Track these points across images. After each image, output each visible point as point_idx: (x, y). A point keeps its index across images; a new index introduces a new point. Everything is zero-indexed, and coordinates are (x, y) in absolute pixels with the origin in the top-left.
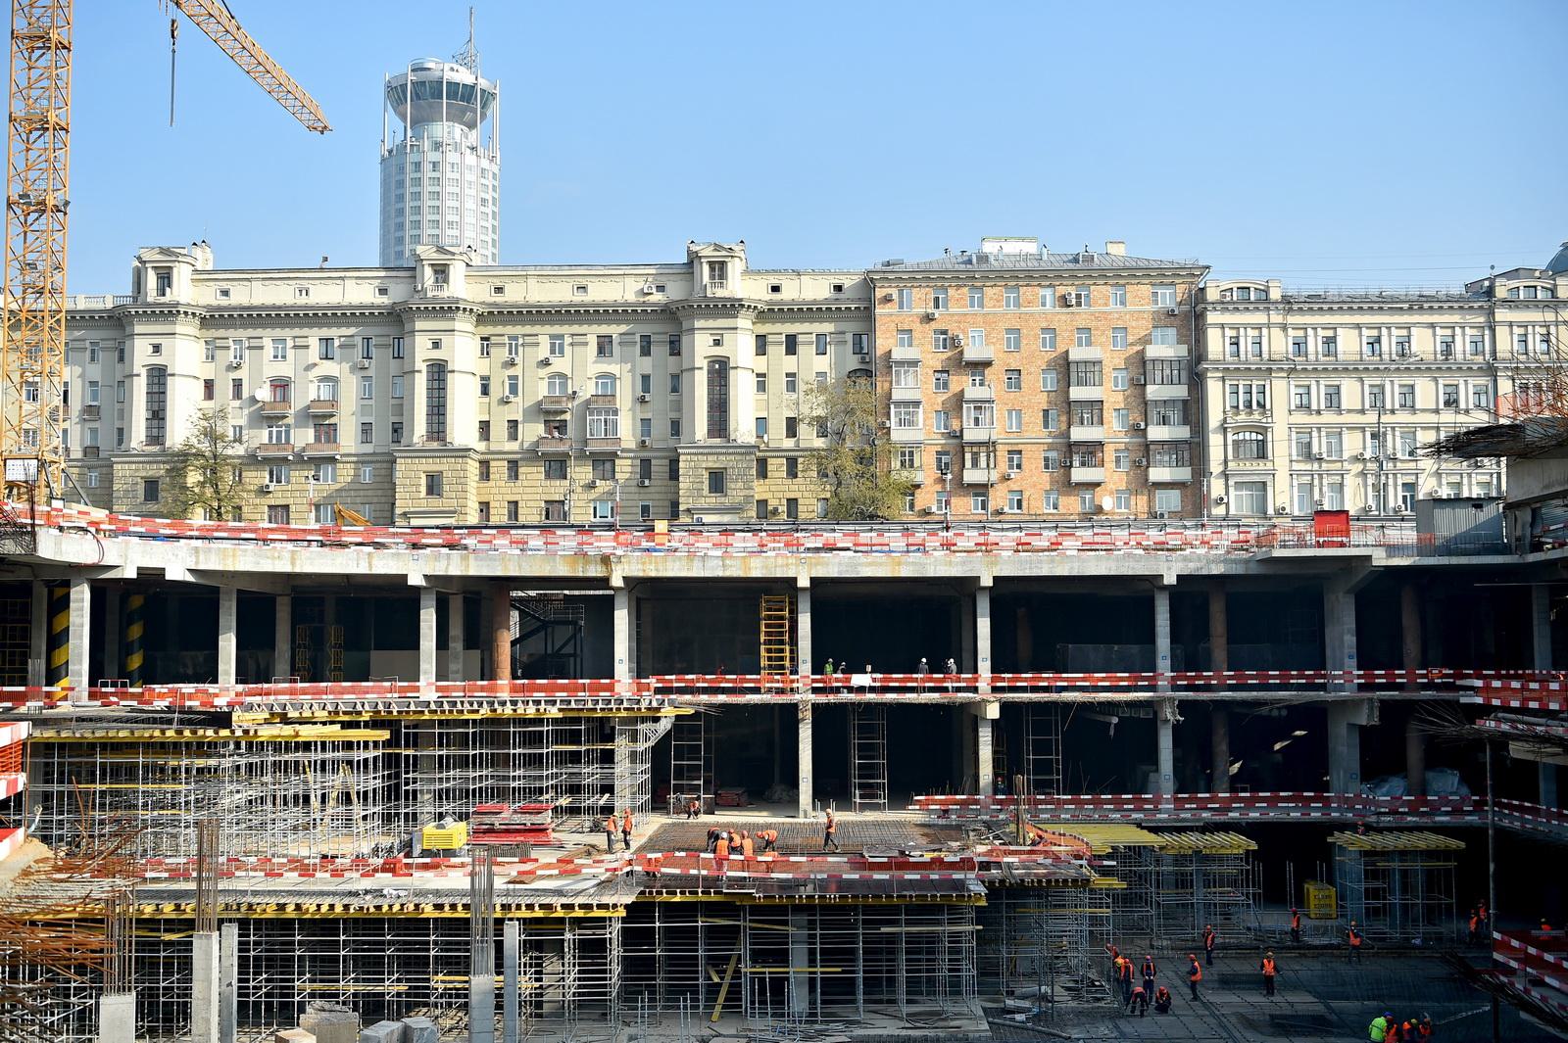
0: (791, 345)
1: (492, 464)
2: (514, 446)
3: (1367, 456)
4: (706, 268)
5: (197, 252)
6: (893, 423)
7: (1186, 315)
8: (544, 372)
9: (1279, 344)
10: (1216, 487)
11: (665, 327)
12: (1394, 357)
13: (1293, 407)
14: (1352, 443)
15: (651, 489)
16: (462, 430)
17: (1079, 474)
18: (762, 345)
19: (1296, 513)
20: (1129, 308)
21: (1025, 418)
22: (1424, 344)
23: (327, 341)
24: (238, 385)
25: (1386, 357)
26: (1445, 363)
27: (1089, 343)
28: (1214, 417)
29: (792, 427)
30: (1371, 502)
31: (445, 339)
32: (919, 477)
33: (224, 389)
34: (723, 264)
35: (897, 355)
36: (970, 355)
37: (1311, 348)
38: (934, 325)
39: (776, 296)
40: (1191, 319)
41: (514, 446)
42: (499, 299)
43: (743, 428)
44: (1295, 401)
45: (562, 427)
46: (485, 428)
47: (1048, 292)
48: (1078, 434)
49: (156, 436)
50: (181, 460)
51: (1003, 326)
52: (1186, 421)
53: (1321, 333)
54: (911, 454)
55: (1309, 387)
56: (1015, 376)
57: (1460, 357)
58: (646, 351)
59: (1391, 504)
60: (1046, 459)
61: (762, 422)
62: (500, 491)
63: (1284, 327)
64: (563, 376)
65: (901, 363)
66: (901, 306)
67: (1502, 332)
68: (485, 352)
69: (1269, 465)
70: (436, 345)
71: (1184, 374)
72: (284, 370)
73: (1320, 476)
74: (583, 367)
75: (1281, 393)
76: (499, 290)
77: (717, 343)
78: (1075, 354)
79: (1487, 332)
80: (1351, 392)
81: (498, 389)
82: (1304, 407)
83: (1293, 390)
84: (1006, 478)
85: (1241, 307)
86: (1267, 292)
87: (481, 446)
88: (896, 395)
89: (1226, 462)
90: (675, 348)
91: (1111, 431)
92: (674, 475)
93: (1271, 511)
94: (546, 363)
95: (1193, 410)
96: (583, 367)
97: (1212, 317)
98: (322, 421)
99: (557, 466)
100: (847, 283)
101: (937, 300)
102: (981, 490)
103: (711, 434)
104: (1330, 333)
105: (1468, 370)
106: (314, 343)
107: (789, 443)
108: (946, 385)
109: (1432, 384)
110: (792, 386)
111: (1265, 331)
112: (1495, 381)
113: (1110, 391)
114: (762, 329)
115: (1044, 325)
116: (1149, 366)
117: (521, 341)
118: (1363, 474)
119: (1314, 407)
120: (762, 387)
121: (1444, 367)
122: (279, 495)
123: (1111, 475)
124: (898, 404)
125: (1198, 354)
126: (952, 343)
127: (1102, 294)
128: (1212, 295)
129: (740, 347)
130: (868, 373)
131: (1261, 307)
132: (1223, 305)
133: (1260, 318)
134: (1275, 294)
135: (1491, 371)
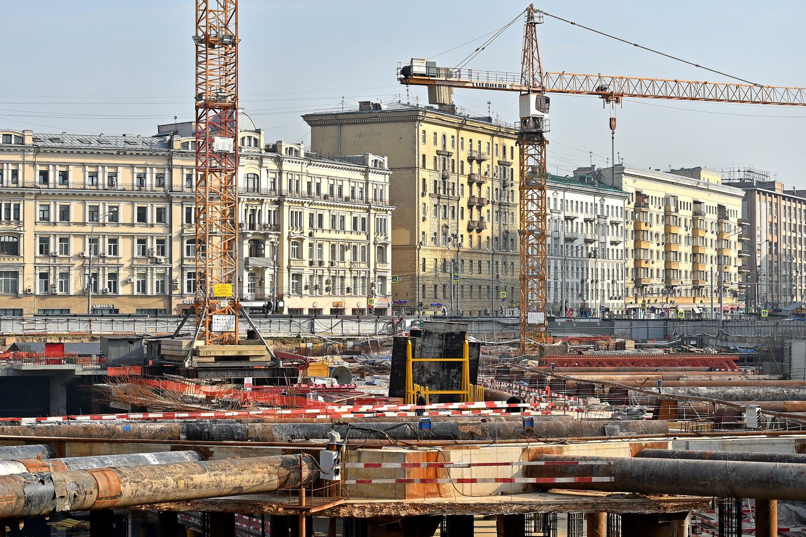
3: (87, 254)
9: (29, 176)
12: (106, 187)
13: (38, 220)
14: (76, 246)
19: (38, 293)
22: (125, 179)
25: (100, 187)
26: (137, 193)
37: (51, 179)
44: (39, 215)
53: (58, 168)
55: (49, 206)
57: (149, 188)
59: (101, 288)
63: (34, 164)
67: (176, 173)
69: (21, 261)
73: (55, 268)
75: (30, 210)
79: (167, 169)
80: (77, 211)
82: (45, 219)
83: (38, 206)
86: (23, 139)
93: (20, 292)
105: (154, 198)
109: (130, 207)
111: (20, 166)
112: (171, 206)
118: (83, 267)
119: (52, 220)
121: (138, 195)
133: (17, 158)
134: (28, 141)
135: (169, 199)
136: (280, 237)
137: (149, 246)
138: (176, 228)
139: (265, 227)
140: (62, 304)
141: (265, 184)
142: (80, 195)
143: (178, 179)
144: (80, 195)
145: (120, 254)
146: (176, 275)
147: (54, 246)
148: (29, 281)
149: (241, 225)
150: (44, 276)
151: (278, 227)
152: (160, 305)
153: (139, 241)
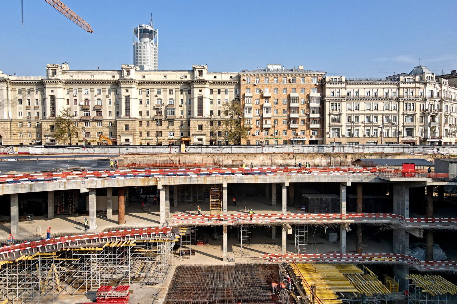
0: (219, 92)
1: (143, 122)
2: (149, 117)
4: (197, 71)
5: (63, 65)
6: (245, 112)
7: (320, 86)
8: (156, 98)
10: (327, 130)
11: (188, 87)
14: (362, 119)
15: (183, 129)
16: (134, 113)
17: (292, 126)
18: (212, 92)
19: (347, 136)
20: (306, 83)
21: (279, 111)
23: (99, 90)
24: (76, 100)
27: (296, 92)
28: (327, 112)
29: (219, 113)
30: (366, 134)
31: (129, 90)
32: (252, 126)
33: (72, 102)
34: (202, 70)
35: (247, 94)
36: (266, 94)
37: (352, 94)
38: (256, 87)
39: (215, 79)
40: (322, 86)
41: (149, 117)
42: (144, 79)
43: (206, 113)
44: (348, 108)
45: (161, 113)
46: (141, 112)
47: (285, 79)
48: (292, 115)
49: (53, 114)
50: (61, 120)
51: (273, 87)
52: (320, 113)
53: (355, 90)
54: (250, 120)
56: (276, 101)
57: (390, 97)
58: (182, 93)
59: (371, 134)
60: (284, 122)
61: (211, 112)
62: (145, 128)
64: (161, 99)
65: (247, 97)
66: (247, 82)
67: (401, 90)
68: (140, 93)
70: (127, 91)
71: (319, 100)
72: (88, 97)
73: (354, 127)
74: (166, 97)
75: (344, 105)
76: (144, 77)
77: (200, 91)
78: (292, 95)
81: (144, 102)
83: (347, 105)
84: (274, 127)
85: (335, 83)
86: (341, 79)
87: (140, 117)
88: (246, 105)
89: (330, 123)
90: (189, 92)
91: (301, 115)
92: (189, 125)
93: (341, 136)
94: (156, 96)
95: (322, 110)
96: (166, 97)
97: (327, 86)
98: (99, 111)
99: (159, 122)
100: (234, 76)
101: (257, 81)
102: (267, 130)
103: (199, 115)
104: (357, 90)
106: (95, 90)
107: (219, 117)
108: (259, 103)
110: (219, 102)
111: (341, 90)
112: (399, 103)
113: (300, 105)
114: (212, 87)
115: (284, 87)
116: (311, 98)
117: (150, 90)
119: (352, 109)
120: (212, 102)
122: (88, 129)
123: (300, 126)
124: (246, 108)
125: (323, 96)
126: (261, 91)
127: (300, 81)
128: (327, 80)
129: (206, 92)
130: (239, 100)
131: (340, 83)
132: (330, 82)
133: (340, 86)
135: (398, 100)
136: (441, 114)
137: (390, 118)
138: (401, 112)
139: (436, 111)
140: (356, 140)
141: (436, 94)
142: (363, 99)
143: (402, 93)
144: (363, 99)
145: (379, 122)
146: (401, 129)
147: (353, 119)
148: (344, 132)
149: (427, 110)
150: (349, 130)
151: (441, 111)
152: (395, 140)
153: (386, 117)
